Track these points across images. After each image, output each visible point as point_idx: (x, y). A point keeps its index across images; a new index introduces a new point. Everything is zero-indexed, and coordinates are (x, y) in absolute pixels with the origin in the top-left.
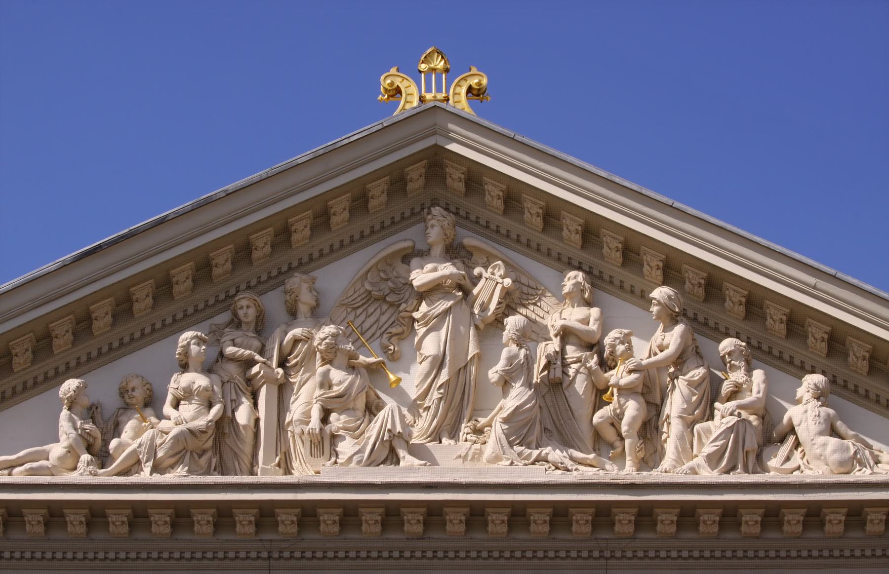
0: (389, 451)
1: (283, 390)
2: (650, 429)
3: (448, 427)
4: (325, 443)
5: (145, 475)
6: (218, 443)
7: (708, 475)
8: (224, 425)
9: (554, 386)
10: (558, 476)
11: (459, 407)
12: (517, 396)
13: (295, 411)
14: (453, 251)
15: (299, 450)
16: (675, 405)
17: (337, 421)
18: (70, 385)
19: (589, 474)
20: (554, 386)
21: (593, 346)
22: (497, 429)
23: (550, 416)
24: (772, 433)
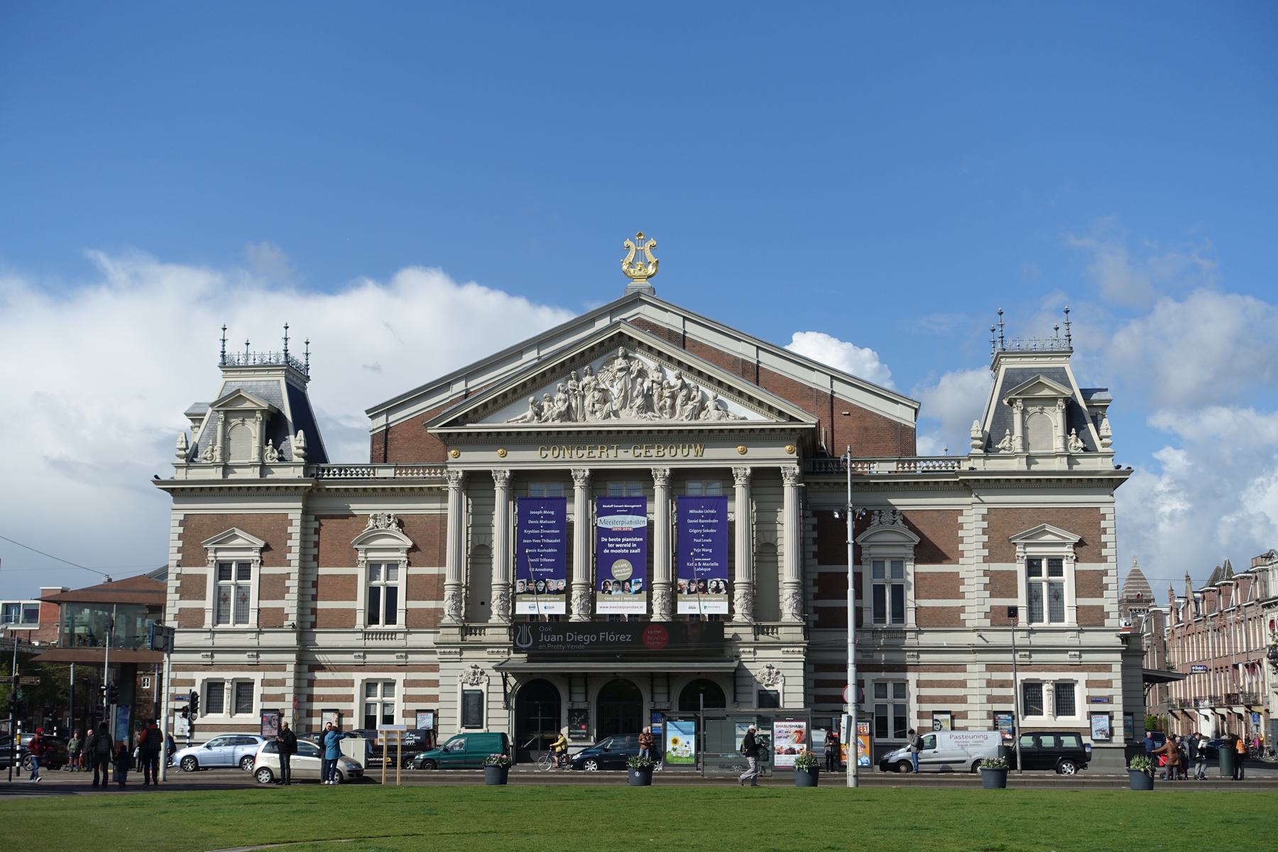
0: (608, 416)
1: (583, 397)
2: (673, 407)
3: (623, 406)
4: (593, 412)
5: (550, 423)
6: (567, 414)
7: (686, 422)
8: (569, 407)
9: (648, 396)
10: (649, 422)
11: (626, 400)
12: (639, 401)
13: (586, 403)
14: (625, 357)
15: (588, 414)
16: (679, 402)
17: (597, 406)
18: (531, 399)
19: (657, 421)
20: (648, 396)
21: (660, 384)
22: (635, 409)
23: (647, 406)
24: (702, 407)
